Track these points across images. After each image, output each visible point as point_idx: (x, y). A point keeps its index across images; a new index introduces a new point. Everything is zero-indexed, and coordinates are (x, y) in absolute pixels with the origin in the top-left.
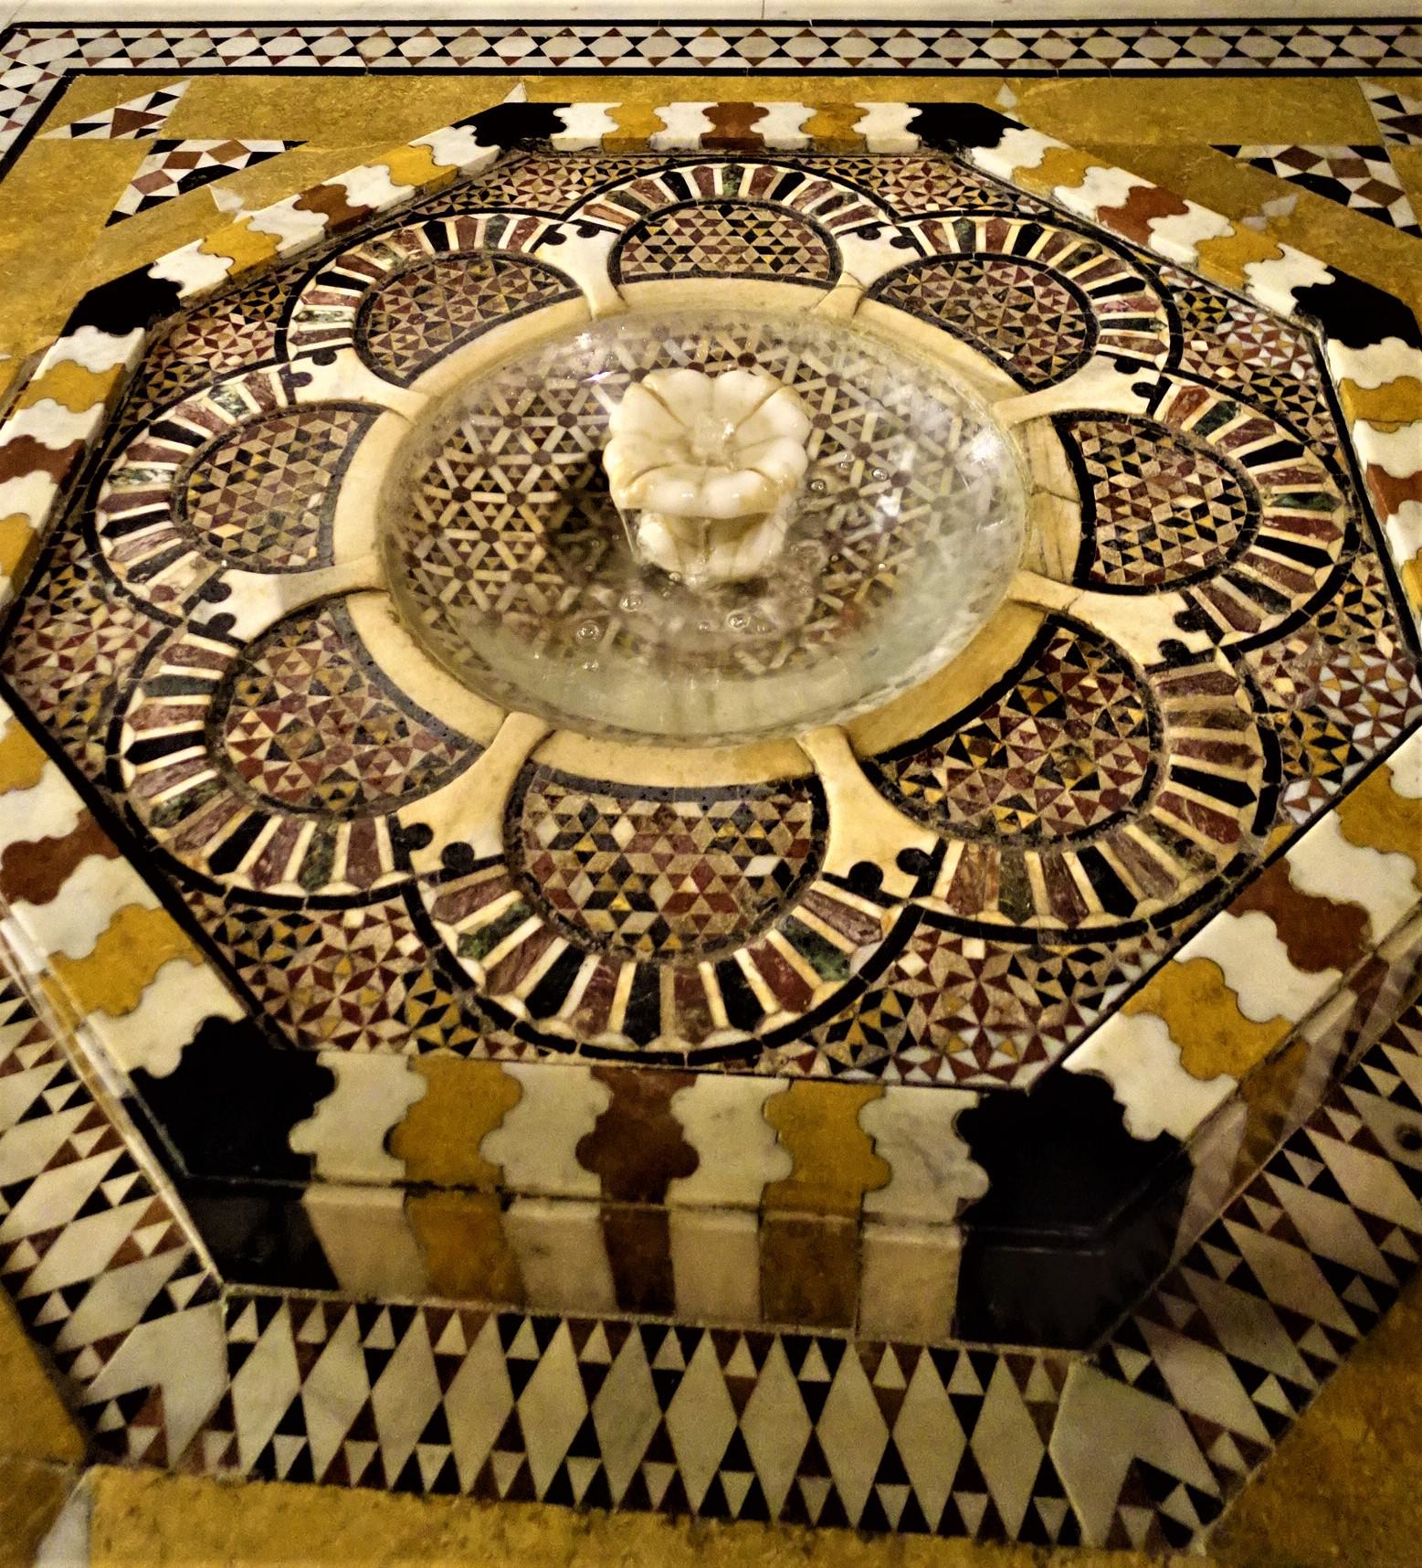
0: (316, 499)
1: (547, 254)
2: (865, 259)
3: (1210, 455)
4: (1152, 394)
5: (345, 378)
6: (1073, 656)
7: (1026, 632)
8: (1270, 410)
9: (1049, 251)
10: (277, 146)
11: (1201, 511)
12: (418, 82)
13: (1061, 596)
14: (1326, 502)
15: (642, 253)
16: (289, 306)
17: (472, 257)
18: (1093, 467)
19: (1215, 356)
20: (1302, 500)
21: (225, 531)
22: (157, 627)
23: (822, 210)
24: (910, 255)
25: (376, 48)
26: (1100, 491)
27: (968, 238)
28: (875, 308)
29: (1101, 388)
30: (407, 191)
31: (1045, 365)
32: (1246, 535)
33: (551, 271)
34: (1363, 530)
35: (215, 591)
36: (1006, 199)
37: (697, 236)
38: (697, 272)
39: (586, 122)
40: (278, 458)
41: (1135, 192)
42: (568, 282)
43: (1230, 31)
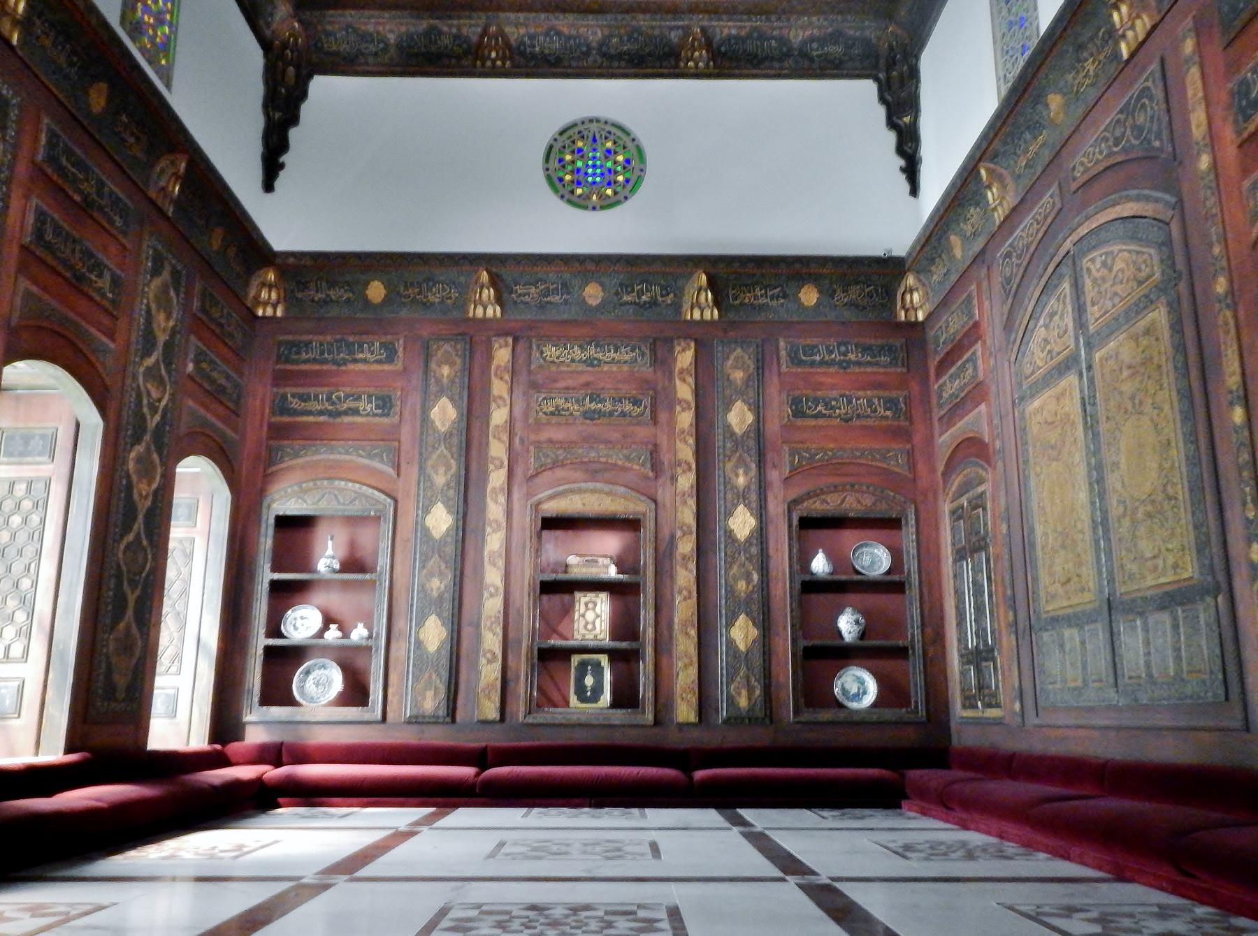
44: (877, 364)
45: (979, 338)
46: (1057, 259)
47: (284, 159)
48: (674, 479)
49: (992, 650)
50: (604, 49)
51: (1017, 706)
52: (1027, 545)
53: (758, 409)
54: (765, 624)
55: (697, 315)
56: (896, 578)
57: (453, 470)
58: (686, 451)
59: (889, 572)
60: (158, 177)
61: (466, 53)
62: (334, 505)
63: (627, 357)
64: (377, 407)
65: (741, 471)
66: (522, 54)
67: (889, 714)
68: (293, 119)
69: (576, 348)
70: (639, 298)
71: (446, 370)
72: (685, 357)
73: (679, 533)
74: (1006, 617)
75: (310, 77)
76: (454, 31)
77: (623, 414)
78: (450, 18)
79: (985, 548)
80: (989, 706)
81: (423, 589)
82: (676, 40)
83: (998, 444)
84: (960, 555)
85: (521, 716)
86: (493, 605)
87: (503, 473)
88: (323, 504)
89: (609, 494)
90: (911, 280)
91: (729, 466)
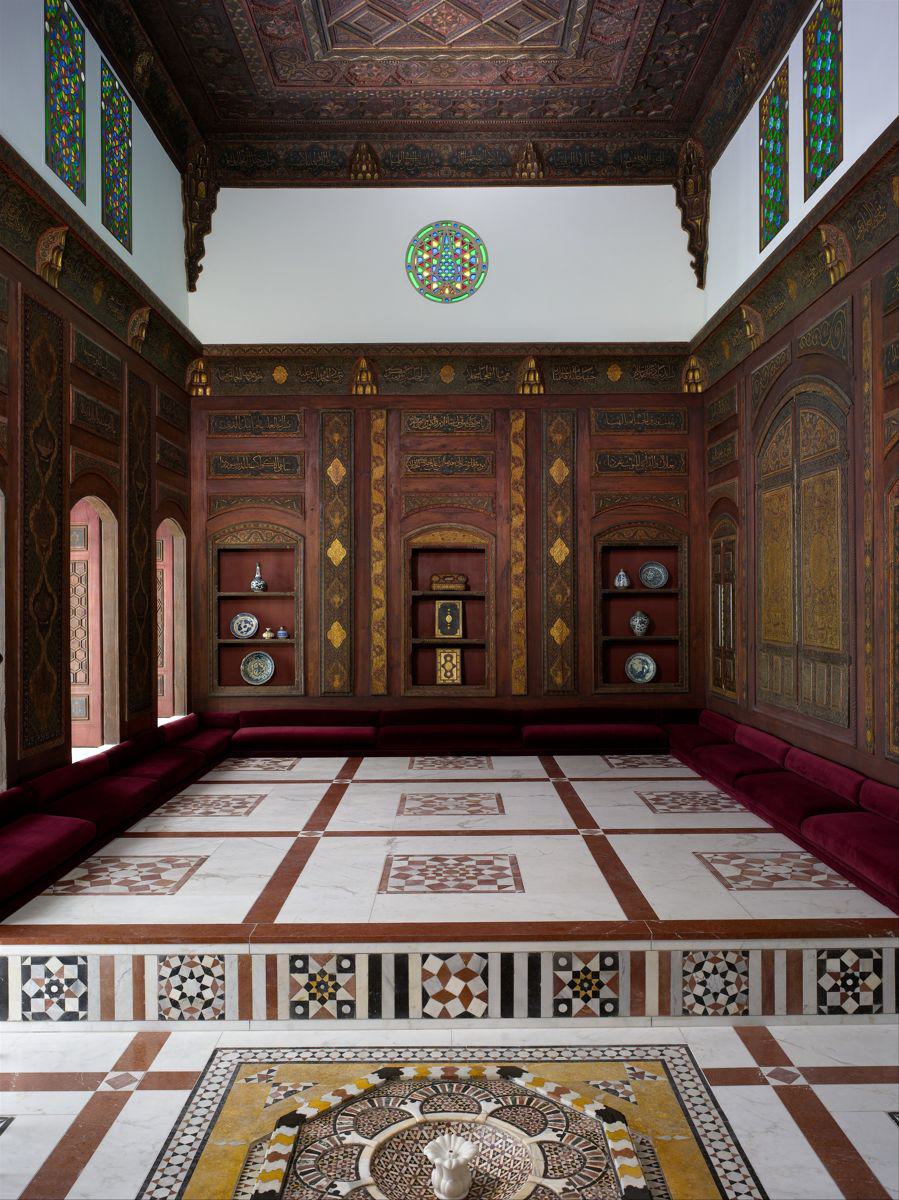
0: (353, 1166)
1: (403, 1107)
2: (488, 1107)
3: (575, 1150)
4: (562, 1136)
5: (353, 1138)
6: (543, 1192)
7: (532, 1188)
8: (590, 1140)
9: (535, 1104)
10: (311, 1084)
11: (573, 1162)
12: (350, 1065)
13: (540, 1180)
14: (602, 1159)
15: (428, 1107)
16: (335, 1121)
17: (382, 1109)
18: (547, 1153)
19: (577, 1128)
20: (596, 1158)
21: (331, 1174)
22: (320, 1194)
23: (475, 1095)
24: (500, 1105)
25: (335, 1055)
26: (549, 1158)
27: (514, 1101)
28: (491, 1119)
29: (549, 1135)
30: (362, 1090)
31: (535, 1131)
32: (583, 1167)
33: (404, 1111)
34: (610, 1164)
35: (333, 1185)
36: (524, 1092)
37: (443, 1102)
38: (443, 1111)
39: (409, 1072)
40: (341, 1157)
41: (557, 1088)
42: (410, 1114)
43: (588, 1049)
44: (665, 428)
45: (735, 427)
46: (786, 399)
47: (201, 262)
48: (509, 520)
49: (732, 653)
50: (454, 161)
51: (744, 695)
52: (757, 591)
53: (572, 464)
54: (575, 626)
55: (527, 391)
56: (672, 590)
57: (346, 515)
58: (519, 498)
59: (665, 586)
60: (133, 330)
61: (341, 166)
62: (260, 541)
63: (473, 425)
64: (287, 467)
65: (559, 512)
66: (387, 166)
67: (660, 687)
68: (206, 228)
69: (435, 418)
70: (483, 377)
71: (336, 437)
72: (518, 425)
73: (513, 560)
74: (742, 633)
75: (218, 189)
76: (332, 147)
77: (471, 470)
78: (328, 138)
79: (731, 581)
80: (729, 689)
81: (328, 602)
82: (512, 153)
83: (744, 512)
84: (717, 581)
85: (402, 691)
86: (379, 614)
87: (382, 516)
88: (252, 540)
89: (460, 530)
90: (693, 362)
91: (550, 508)
